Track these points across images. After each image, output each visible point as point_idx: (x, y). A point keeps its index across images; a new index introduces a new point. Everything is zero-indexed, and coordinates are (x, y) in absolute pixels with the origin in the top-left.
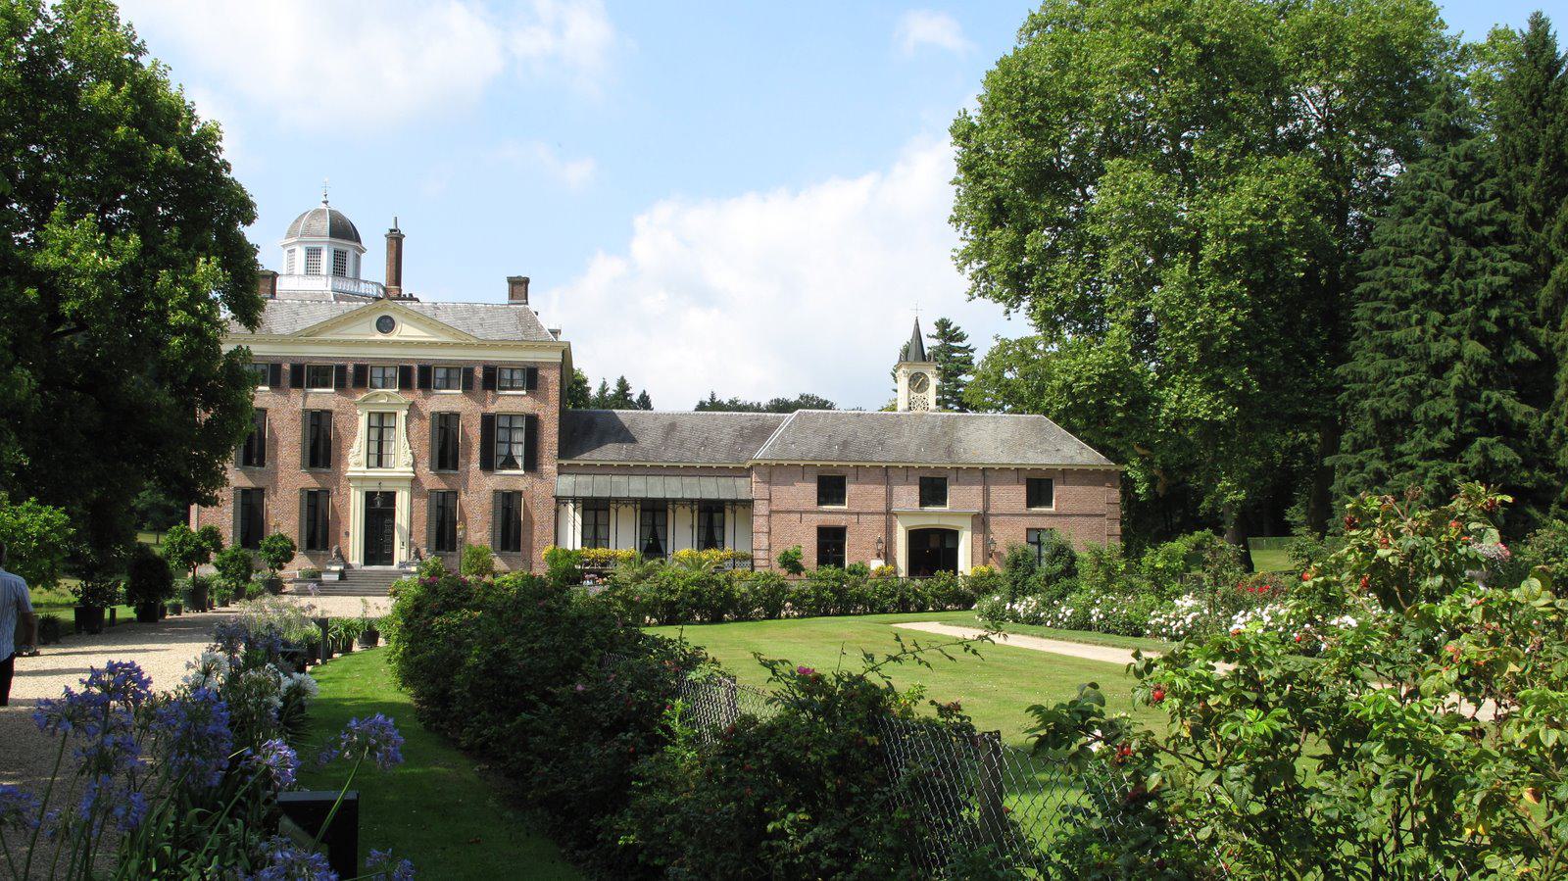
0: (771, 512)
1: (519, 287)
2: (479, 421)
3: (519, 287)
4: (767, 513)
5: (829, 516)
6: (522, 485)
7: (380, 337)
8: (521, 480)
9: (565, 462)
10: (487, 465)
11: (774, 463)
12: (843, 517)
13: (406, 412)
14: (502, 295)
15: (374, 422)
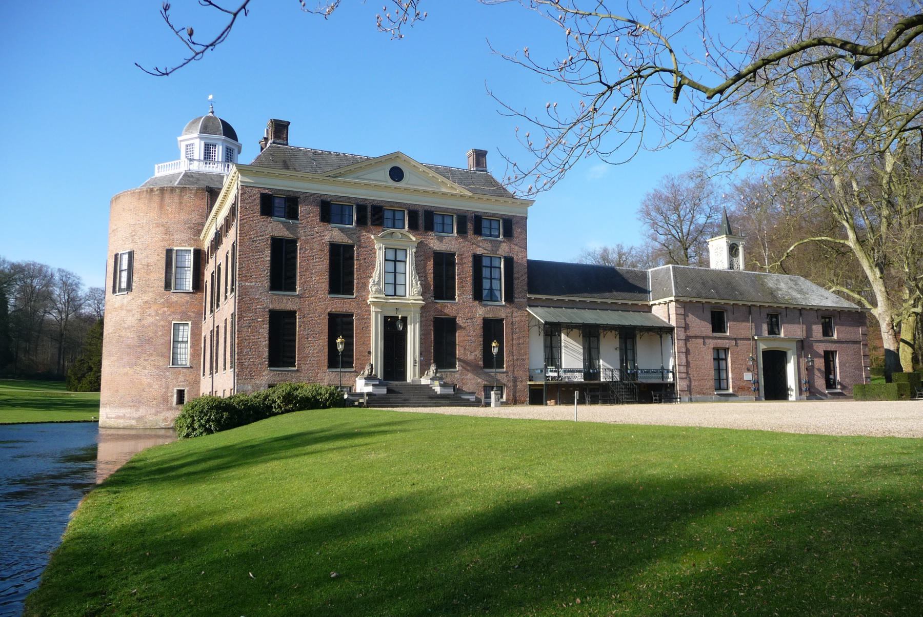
0: (687, 336)
1: (480, 156)
2: (471, 260)
3: (480, 156)
4: (684, 338)
5: (719, 341)
6: (502, 314)
7: (391, 183)
8: (503, 310)
9: (533, 296)
10: (478, 295)
11: (688, 300)
12: (727, 341)
13: (414, 250)
14: (466, 163)
15: (391, 256)
